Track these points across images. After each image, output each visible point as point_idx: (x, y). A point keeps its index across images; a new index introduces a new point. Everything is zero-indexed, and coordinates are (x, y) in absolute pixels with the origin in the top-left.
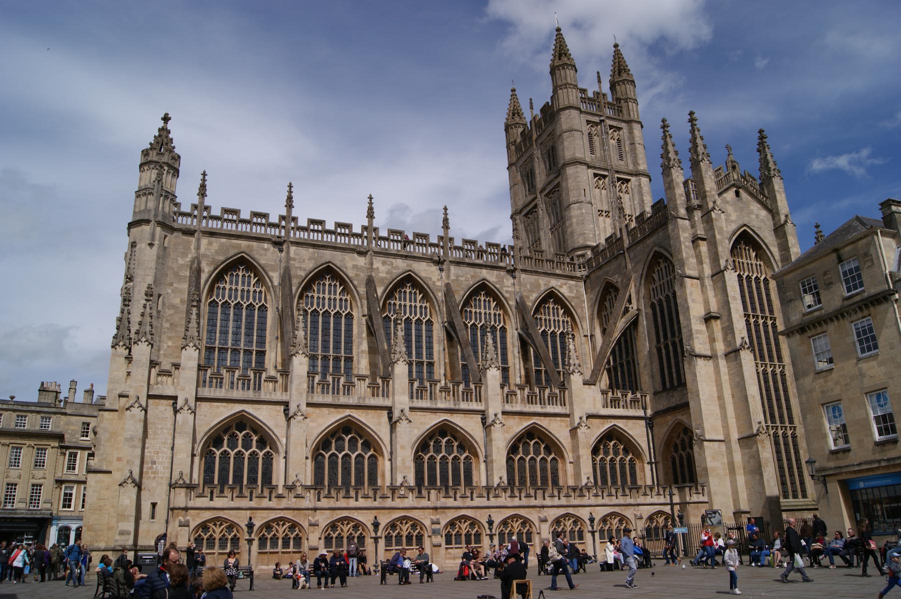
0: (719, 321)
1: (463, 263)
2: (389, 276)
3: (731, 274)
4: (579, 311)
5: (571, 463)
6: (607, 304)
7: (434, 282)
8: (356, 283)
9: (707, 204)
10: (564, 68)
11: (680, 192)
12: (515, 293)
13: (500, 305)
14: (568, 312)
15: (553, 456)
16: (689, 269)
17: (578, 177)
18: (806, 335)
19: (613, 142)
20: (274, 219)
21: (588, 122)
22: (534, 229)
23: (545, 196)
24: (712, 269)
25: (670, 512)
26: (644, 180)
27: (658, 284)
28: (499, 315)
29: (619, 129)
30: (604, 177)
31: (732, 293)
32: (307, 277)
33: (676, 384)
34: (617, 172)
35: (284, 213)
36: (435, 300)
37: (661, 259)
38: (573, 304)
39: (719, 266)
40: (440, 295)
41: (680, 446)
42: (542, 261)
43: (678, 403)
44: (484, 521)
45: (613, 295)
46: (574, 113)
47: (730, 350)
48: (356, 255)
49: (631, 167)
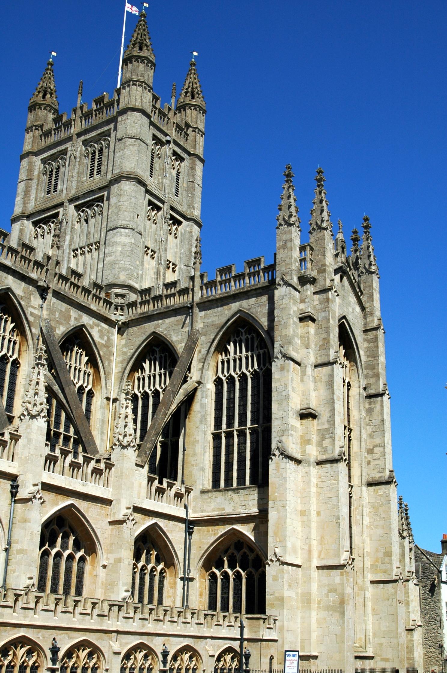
0: (315, 421)
3: (338, 369)
4: (106, 364)
5: (104, 567)
6: (146, 365)
9: (325, 280)
11: (296, 257)
14: (93, 362)
15: (81, 553)
16: (293, 350)
17: (135, 197)
19: (174, 172)
21: (155, 137)
24: (316, 358)
25: (238, 649)
26: (196, 229)
28: (15, 343)
29: (182, 159)
30: (159, 209)
31: (338, 390)
37: (243, 328)
38: (101, 354)
39: (328, 356)
42: (78, 287)
44: (46, 647)
47: (324, 457)
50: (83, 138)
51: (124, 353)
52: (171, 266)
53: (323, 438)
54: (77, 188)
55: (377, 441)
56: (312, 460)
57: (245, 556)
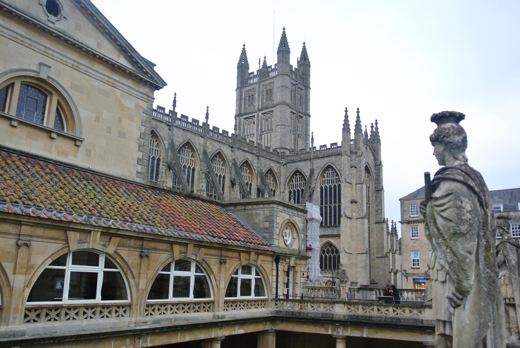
1: (241, 149)
2: (212, 151)
6: (294, 180)
7: (229, 158)
8: (199, 152)
10: (286, 52)
12: (258, 167)
13: (251, 172)
14: (275, 180)
18: (409, 225)
19: (299, 96)
20: (167, 112)
22: (250, 128)
23: (262, 114)
27: (326, 179)
29: (302, 89)
32: (180, 145)
33: (328, 225)
34: (299, 112)
35: (172, 109)
36: (228, 166)
37: (330, 168)
39: (361, 181)
40: (230, 164)
41: (326, 252)
43: (330, 234)
45: (298, 176)
46: (288, 78)
47: (360, 217)
48: (200, 138)
49: (304, 111)
50: (262, 84)
51: (286, 175)
52: (300, 136)
53: (359, 210)
54: (262, 105)
55: (379, 208)
56: (355, 218)
57: (332, 250)
